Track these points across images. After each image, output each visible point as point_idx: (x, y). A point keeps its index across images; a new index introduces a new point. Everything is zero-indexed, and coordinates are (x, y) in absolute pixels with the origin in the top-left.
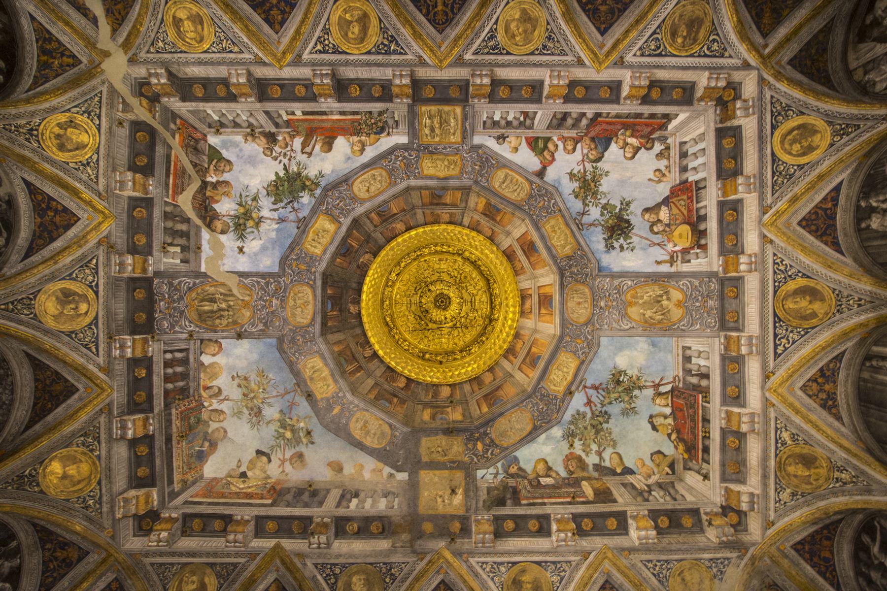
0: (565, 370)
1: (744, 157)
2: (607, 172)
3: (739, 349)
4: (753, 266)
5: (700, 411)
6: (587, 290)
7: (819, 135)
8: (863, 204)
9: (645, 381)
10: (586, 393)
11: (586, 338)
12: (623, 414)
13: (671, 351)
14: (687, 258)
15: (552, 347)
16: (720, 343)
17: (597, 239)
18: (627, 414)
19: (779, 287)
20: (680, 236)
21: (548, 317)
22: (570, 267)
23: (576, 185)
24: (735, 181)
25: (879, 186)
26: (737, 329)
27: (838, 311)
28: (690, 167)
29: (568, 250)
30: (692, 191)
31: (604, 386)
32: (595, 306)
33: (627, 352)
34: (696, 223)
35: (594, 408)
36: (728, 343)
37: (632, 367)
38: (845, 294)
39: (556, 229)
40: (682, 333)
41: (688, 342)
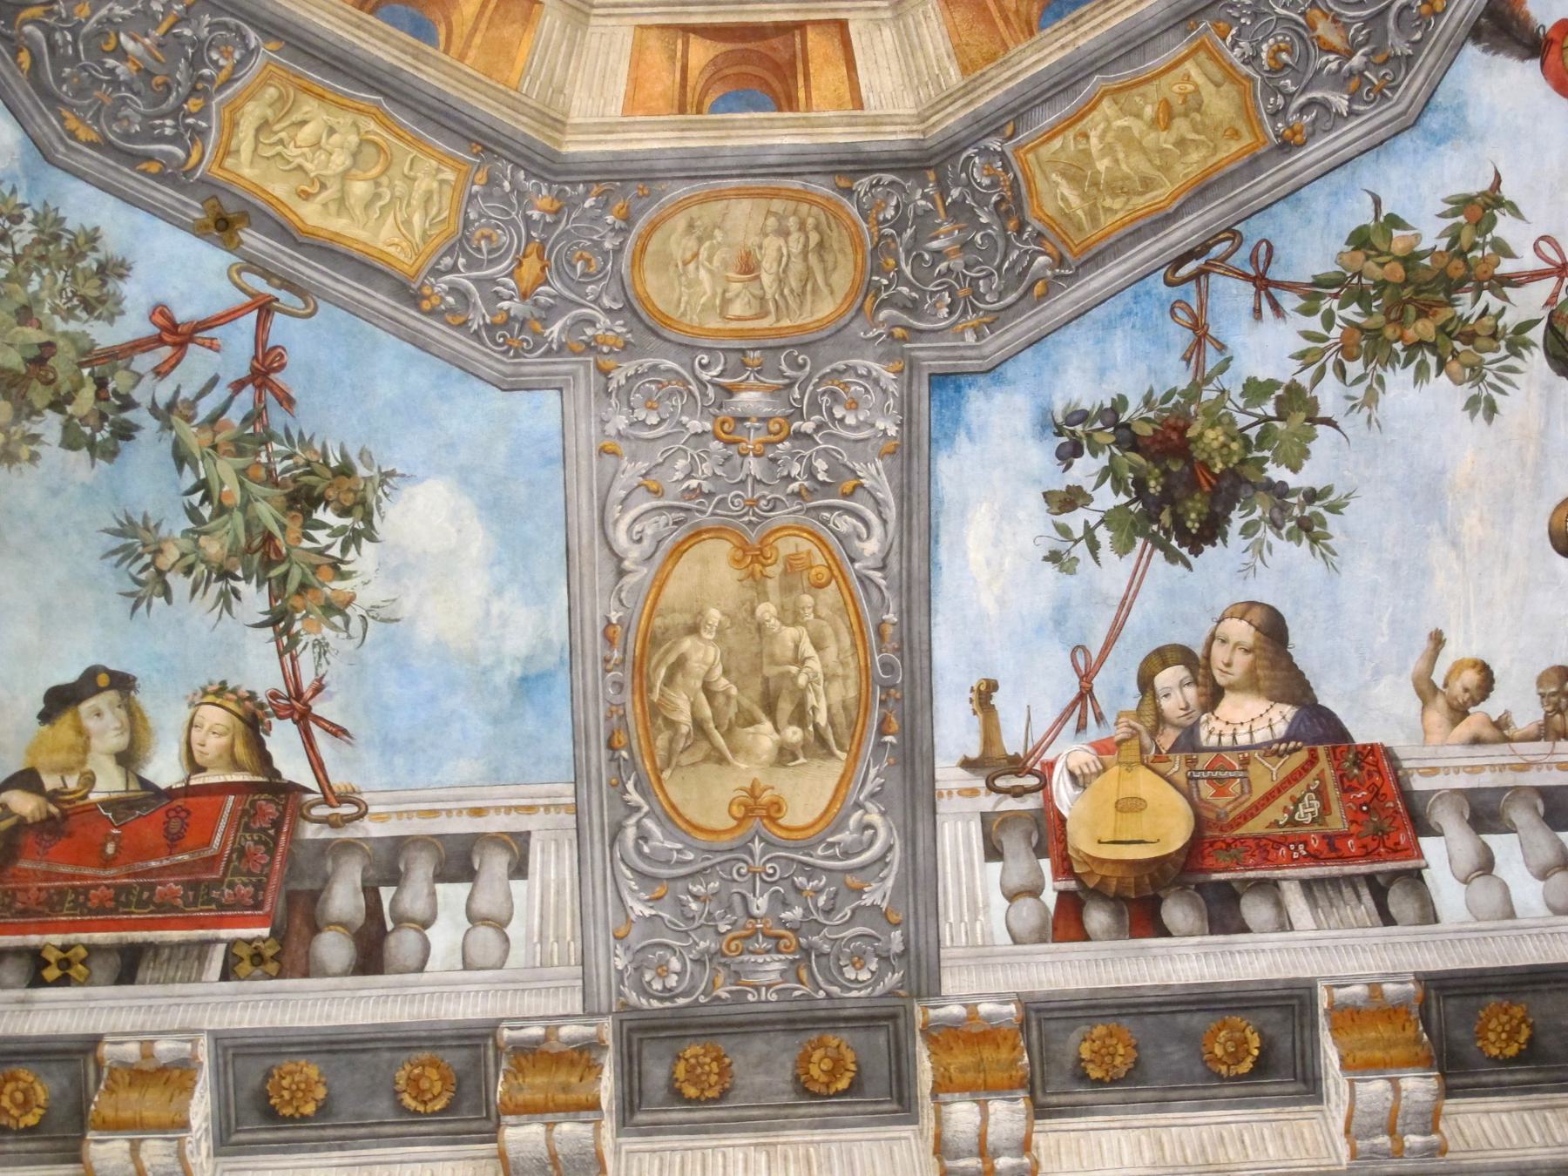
0: (360, 189)
1: (1533, 1100)
2: (1492, 409)
3: (530, 1110)
4: (973, 1163)
5: (175, 935)
6: (826, 308)
9: (322, 648)
10: (231, 316)
11: (549, 313)
12: (126, 529)
13: (496, 776)
14: (1014, 844)
15: (486, 107)
16: (553, 1022)
17: (1115, 362)
18: (128, 554)
20: (1130, 806)
21: (663, 81)
22: (958, 211)
23: (1430, 233)
24: (1410, 1063)
26: (631, 1103)
28: (1493, 840)
29: (1056, 196)
30: (1368, 854)
31: (277, 418)
32: (738, 360)
33: (478, 540)
34: (1203, 878)
35: (144, 362)
36: (558, 1060)
37: (396, 575)
39: (1181, 126)
40: (600, 829)
41: (552, 863)
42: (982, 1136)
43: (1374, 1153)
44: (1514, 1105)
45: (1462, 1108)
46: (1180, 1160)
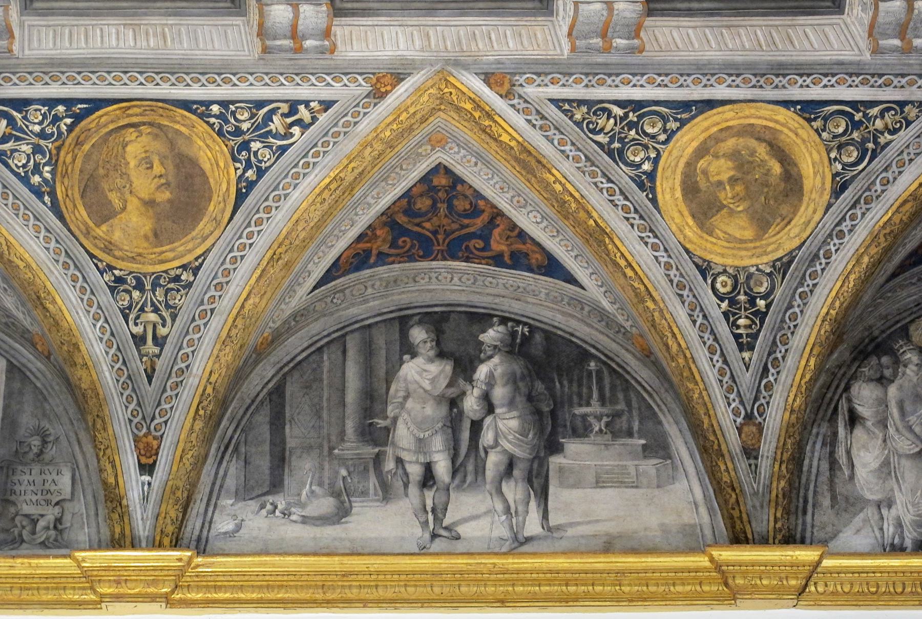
1: (715, 21)
7: (748, 234)
8: (492, 335)
19: (201, 116)
25: (540, 386)
27: (120, 280)
38: (177, 300)
42: (294, 27)
43: (589, 49)
44: (699, 24)
45: (658, 23)
46: (442, 48)
